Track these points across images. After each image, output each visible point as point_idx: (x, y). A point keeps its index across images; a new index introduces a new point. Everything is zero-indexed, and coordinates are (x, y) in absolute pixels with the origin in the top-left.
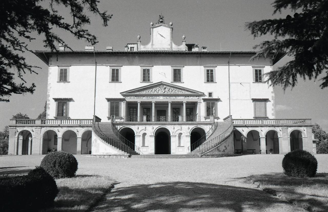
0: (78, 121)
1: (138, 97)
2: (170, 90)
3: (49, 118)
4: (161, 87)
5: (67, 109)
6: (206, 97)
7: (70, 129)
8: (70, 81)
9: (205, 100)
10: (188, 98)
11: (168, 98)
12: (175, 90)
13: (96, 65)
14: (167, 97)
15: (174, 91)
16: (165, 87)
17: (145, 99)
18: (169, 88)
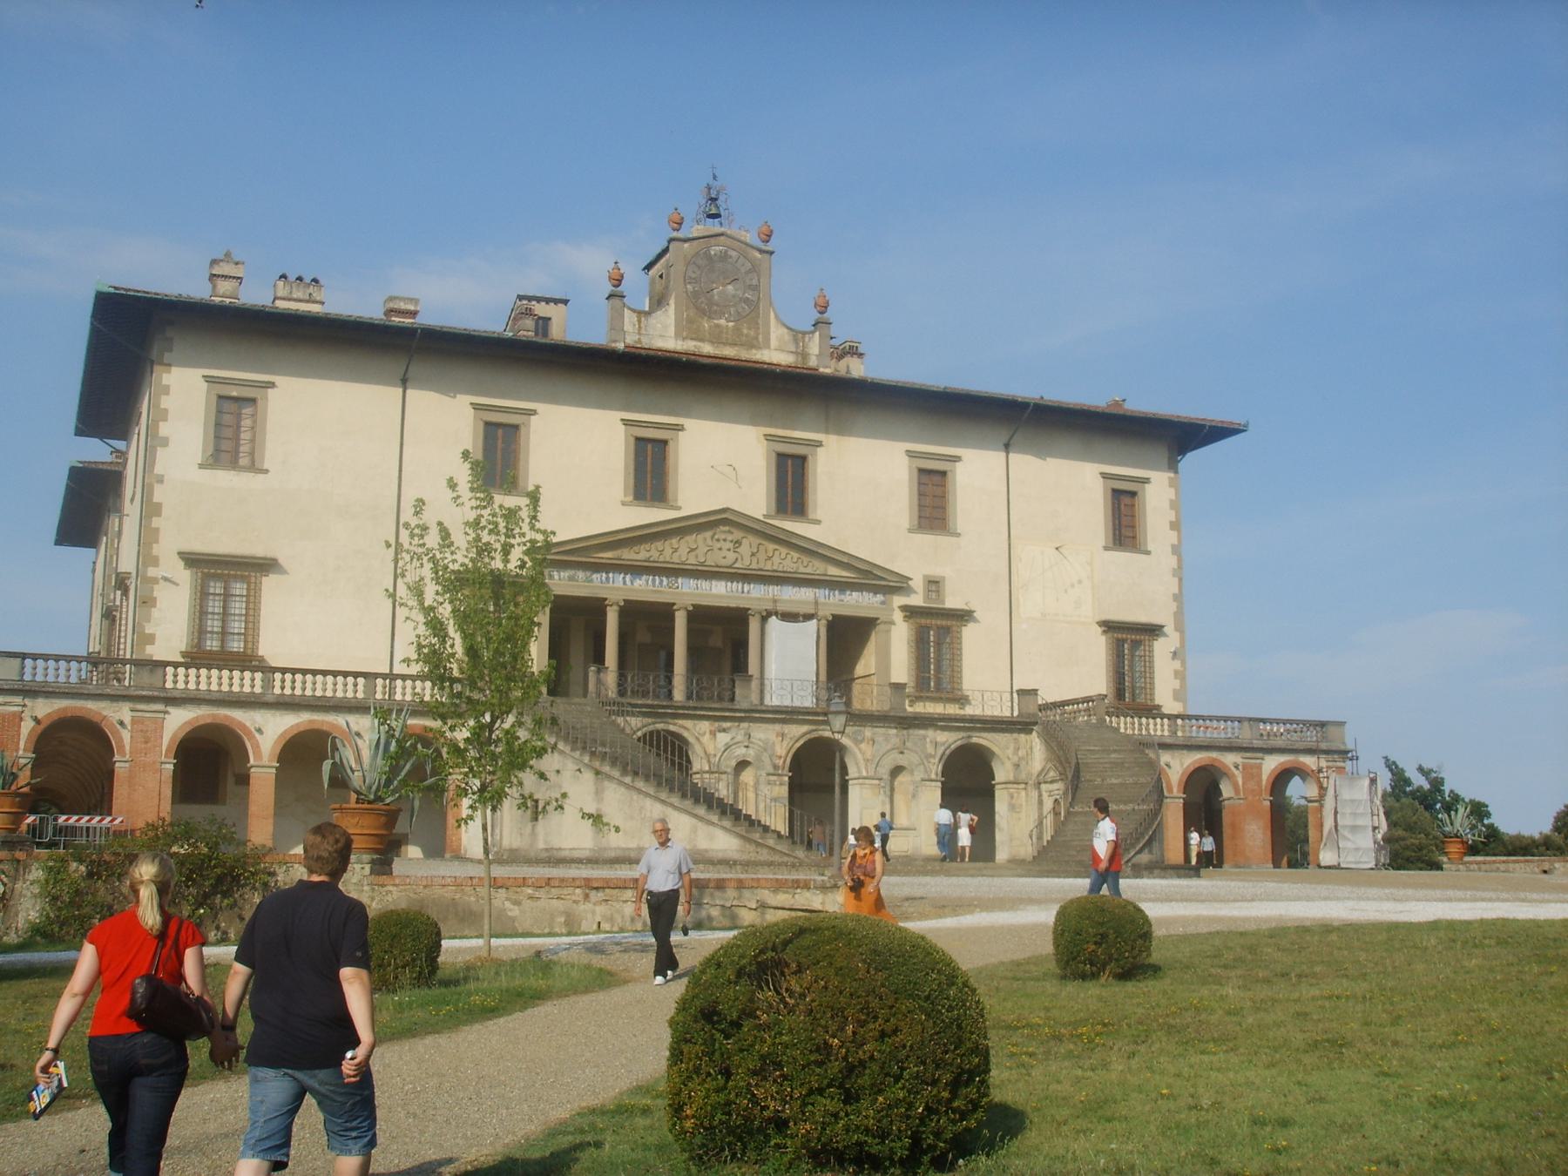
0: (361, 681)
1: (607, 578)
2: (762, 556)
3: (152, 656)
4: (723, 537)
5: (956, 656)
6: (913, 596)
7: (1214, 755)
8: (265, 467)
9: (911, 612)
10: (843, 597)
11: (748, 592)
12: (783, 556)
13: (1008, 453)
14: (743, 588)
15: (776, 560)
16: (738, 534)
17: (644, 588)
18: (755, 540)
